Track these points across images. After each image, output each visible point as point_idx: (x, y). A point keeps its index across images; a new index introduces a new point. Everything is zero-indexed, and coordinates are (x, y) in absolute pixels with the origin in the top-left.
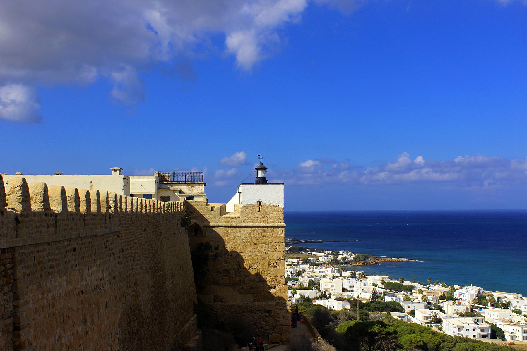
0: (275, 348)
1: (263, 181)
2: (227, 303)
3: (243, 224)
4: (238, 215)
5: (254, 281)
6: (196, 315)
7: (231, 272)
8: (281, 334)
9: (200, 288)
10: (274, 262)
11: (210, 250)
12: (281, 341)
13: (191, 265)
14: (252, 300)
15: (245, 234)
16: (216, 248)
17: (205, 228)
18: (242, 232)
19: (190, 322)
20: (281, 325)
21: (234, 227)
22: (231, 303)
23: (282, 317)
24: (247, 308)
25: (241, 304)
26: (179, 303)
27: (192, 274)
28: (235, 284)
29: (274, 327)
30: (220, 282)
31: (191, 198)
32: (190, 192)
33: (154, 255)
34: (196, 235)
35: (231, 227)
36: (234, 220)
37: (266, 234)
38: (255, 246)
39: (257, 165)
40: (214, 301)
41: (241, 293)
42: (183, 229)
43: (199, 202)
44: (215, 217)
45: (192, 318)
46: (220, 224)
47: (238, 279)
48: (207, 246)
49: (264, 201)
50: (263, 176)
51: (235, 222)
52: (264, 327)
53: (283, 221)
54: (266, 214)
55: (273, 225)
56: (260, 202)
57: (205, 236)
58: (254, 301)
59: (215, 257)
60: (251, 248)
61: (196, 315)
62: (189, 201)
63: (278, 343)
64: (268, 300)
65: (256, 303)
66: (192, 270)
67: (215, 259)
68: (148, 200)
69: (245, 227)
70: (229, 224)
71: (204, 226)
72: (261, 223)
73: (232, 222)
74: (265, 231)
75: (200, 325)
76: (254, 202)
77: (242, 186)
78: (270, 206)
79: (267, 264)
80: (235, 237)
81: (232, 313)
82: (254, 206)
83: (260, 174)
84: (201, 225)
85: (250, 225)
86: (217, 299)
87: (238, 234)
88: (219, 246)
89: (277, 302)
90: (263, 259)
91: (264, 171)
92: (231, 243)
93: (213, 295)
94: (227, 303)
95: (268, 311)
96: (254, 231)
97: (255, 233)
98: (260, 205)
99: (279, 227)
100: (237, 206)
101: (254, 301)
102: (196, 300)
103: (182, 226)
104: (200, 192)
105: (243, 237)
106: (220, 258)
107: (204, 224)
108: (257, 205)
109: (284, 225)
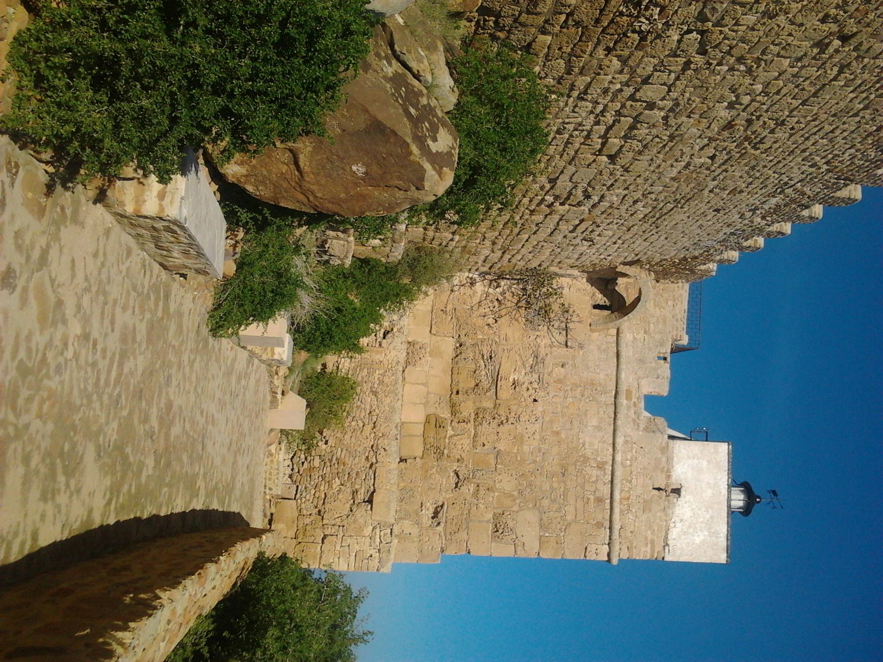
10: (511, 524)
15: (591, 444)
37: (592, 504)
38: (557, 469)
41: (427, 421)
53: (625, 555)
54: (646, 506)
55: (617, 527)
56: (677, 491)
65: (394, 465)
73: (628, 408)
81: (375, 393)
85: (619, 458)
95: (370, 501)
97: (595, 472)
109: (615, 561)
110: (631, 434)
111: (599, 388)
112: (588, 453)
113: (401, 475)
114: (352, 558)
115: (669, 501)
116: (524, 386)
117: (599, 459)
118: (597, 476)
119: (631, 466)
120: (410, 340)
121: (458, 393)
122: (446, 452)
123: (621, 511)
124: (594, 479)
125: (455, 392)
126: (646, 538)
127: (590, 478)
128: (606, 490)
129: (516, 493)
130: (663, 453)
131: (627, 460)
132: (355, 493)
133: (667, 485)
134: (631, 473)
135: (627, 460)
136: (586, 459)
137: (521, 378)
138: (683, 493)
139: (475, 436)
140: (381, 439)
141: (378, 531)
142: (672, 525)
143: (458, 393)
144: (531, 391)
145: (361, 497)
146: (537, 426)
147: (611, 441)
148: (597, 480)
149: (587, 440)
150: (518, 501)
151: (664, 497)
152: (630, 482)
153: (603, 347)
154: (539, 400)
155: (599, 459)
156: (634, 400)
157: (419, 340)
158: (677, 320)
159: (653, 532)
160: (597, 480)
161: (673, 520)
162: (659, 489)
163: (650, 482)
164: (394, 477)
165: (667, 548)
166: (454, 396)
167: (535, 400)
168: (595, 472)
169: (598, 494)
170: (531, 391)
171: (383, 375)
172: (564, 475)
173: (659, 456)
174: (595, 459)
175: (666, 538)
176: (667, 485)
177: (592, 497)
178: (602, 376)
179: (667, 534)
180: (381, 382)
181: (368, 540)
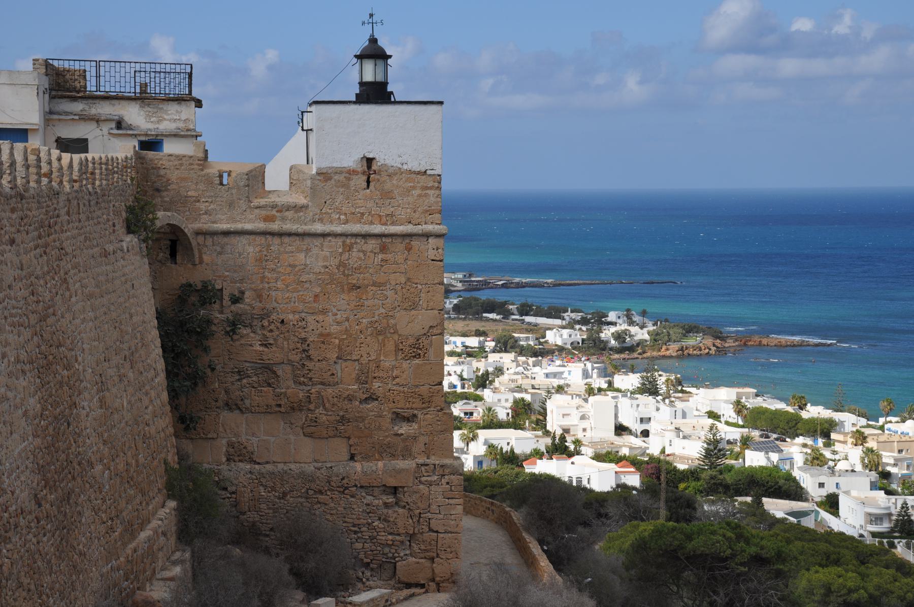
0: (414, 601)
1: (375, 93)
2: (269, 467)
3: (318, 228)
4: (302, 200)
5: (350, 399)
6: (172, 504)
7: (280, 373)
8: (432, 559)
9: (186, 423)
10: (411, 341)
11: (216, 306)
12: (433, 580)
13: (157, 351)
14: (347, 457)
15: (325, 259)
16: (235, 300)
17: (201, 239)
18: (315, 251)
19: (155, 523)
20: (431, 530)
21: (290, 234)
22: (280, 466)
23: (434, 507)
24: (329, 482)
25: (310, 468)
26: (121, 467)
27: (162, 378)
28: (293, 409)
29: (412, 537)
30: (247, 402)
31: (151, 144)
32: (150, 126)
33: (43, 319)
34: (173, 255)
35: (281, 234)
36: (290, 214)
37: (389, 256)
38: (354, 293)
39: (360, 43)
40: (228, 460)
41: (310, 435)
42: (130, 240)
43: (180, 158)
44: (231, 205)
45: (162, 513)
46: (248, 226)
47: (301, 395)
48: (207, 294)
49: (386, 157)
50: (380, 78)
51: (293, 221)
52: (383, 537)
54: (387, 195)
56: (370, 161)
57: (201, 262)
58: (352, 458)
59: (233, 326)
60: (342, 302)
61: (172, 504)
62: (150, 154)
63: (423, 586)
64: (393, 456)
65: (358, 466)
66: (161, 365)
67: (234, 331)
68: (19, 146)
69: (324, 235)
70: (275, 226)
71: (198, 233)
72: (372, 223)
73: (283, 219)
74: (384, 249)
75: (185, 532)
76: (350, 160)
77: (313, 108)
78: (399, 172)
79: (390, 346)
80: (293, 266)
81: (285, 494)
82: (351, 172)
83: (370, 72)
84: (189, 228)
85: (339, 229)
86: (237, 453)
87: (302, 256)
88: (243, 293)
89: (421, 461)
90: (379, 333)
91: (380, 63)
92: (280, 284)
93: (224, 441)
94: (269, 467)
95: (395, 490)
96: (350, 248)
97: (355, 254)
98: (369, 167)
99: (427, 235)
100: (300, 171)
101: (352, 458)
102: (172, 458)
103: (129, 231)
104: (181, 125)
105: (318, 266)
106: (244, 331)
107: (197, 226)
108: (362, 167)
110: (311, 214)
111: (265, 253)
112: (334, 262)
113: (367, 458)
114: (451, 501)
115: (380, 171)
116: (268, 334)
117: (340, 250)
118: (359, 251)
119: (345, 214)
120: (224, 459)
121: (280, 406)
122: (341, 413)
123: (393, 224)
124: (361, 255)
125: (278, 409)
126: (420, 196)
127: (360, 258)
128: (372, 244)
129: (381, 338)
130: (330, 179)
131: (339, 218)
132: (386, 505)
133: (364, 173)
134: (353, 213)
135: (339, 218)
136: (341, 264)
137: (258, 338)
138: (371, 156)
139: (322, 384)
140: (333, 484)
141: (423, 479)
142: (405, 167)
143: (280, 406)
144: (272, 327)
145: (391, 500)
146: (310, 318)
147: (320, 240)
148: (363, 251)
149: (321, 264)
150: (389, 335)
151: (377, 177)
152: (363, 214)
153: (218, 249)
154: (282, 317)
155: (340, 250)
156: (274, 212)
157: (224, 449)
158: (181, 165)
159: (414, 188)
160: (363, 251)
161: (400, 166)
162: (368, 182)
163: (362, 192)
164: (370, 466)
165: (429, 172)
166: (283, 410)
167: (283, 321)
168: (354, 254)
169: (377, 250)
170: (272, 327)
171: (265, 487)
172: (359, 287)
173: (333, 182)
174: (341, 254)
175: (419, 173)
176: (364, 173)
177: (380, 256)
178: (251, 249)
179: (415, 173)
180: (273, 489)
181: (432, 488)
